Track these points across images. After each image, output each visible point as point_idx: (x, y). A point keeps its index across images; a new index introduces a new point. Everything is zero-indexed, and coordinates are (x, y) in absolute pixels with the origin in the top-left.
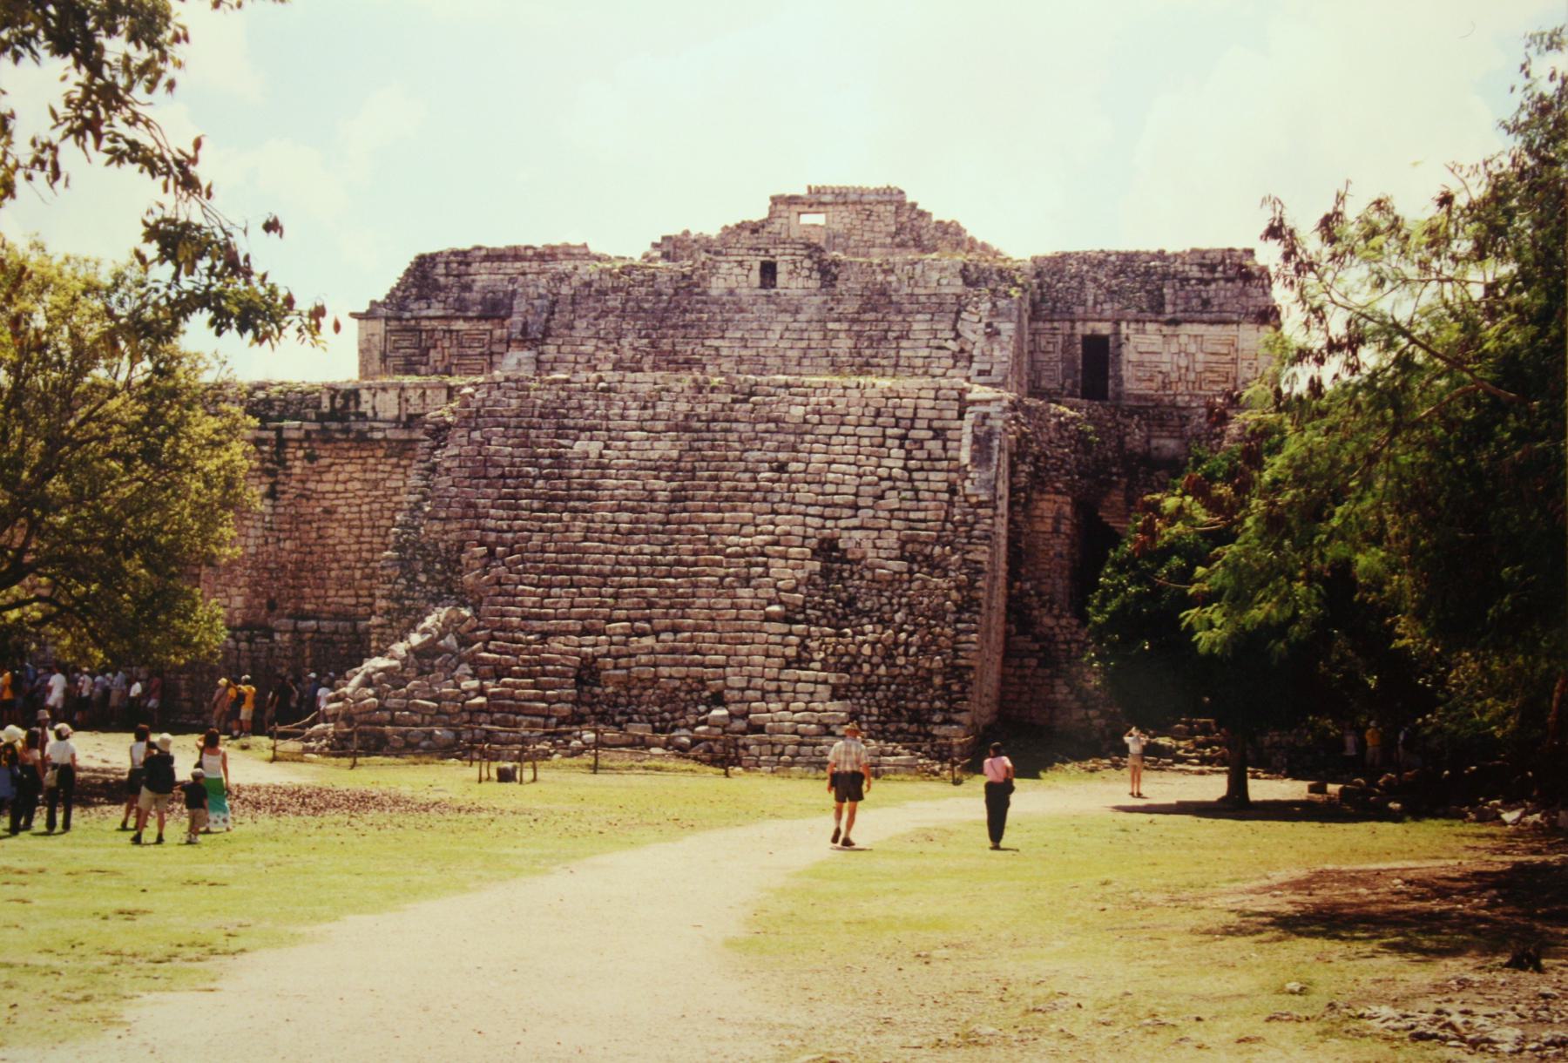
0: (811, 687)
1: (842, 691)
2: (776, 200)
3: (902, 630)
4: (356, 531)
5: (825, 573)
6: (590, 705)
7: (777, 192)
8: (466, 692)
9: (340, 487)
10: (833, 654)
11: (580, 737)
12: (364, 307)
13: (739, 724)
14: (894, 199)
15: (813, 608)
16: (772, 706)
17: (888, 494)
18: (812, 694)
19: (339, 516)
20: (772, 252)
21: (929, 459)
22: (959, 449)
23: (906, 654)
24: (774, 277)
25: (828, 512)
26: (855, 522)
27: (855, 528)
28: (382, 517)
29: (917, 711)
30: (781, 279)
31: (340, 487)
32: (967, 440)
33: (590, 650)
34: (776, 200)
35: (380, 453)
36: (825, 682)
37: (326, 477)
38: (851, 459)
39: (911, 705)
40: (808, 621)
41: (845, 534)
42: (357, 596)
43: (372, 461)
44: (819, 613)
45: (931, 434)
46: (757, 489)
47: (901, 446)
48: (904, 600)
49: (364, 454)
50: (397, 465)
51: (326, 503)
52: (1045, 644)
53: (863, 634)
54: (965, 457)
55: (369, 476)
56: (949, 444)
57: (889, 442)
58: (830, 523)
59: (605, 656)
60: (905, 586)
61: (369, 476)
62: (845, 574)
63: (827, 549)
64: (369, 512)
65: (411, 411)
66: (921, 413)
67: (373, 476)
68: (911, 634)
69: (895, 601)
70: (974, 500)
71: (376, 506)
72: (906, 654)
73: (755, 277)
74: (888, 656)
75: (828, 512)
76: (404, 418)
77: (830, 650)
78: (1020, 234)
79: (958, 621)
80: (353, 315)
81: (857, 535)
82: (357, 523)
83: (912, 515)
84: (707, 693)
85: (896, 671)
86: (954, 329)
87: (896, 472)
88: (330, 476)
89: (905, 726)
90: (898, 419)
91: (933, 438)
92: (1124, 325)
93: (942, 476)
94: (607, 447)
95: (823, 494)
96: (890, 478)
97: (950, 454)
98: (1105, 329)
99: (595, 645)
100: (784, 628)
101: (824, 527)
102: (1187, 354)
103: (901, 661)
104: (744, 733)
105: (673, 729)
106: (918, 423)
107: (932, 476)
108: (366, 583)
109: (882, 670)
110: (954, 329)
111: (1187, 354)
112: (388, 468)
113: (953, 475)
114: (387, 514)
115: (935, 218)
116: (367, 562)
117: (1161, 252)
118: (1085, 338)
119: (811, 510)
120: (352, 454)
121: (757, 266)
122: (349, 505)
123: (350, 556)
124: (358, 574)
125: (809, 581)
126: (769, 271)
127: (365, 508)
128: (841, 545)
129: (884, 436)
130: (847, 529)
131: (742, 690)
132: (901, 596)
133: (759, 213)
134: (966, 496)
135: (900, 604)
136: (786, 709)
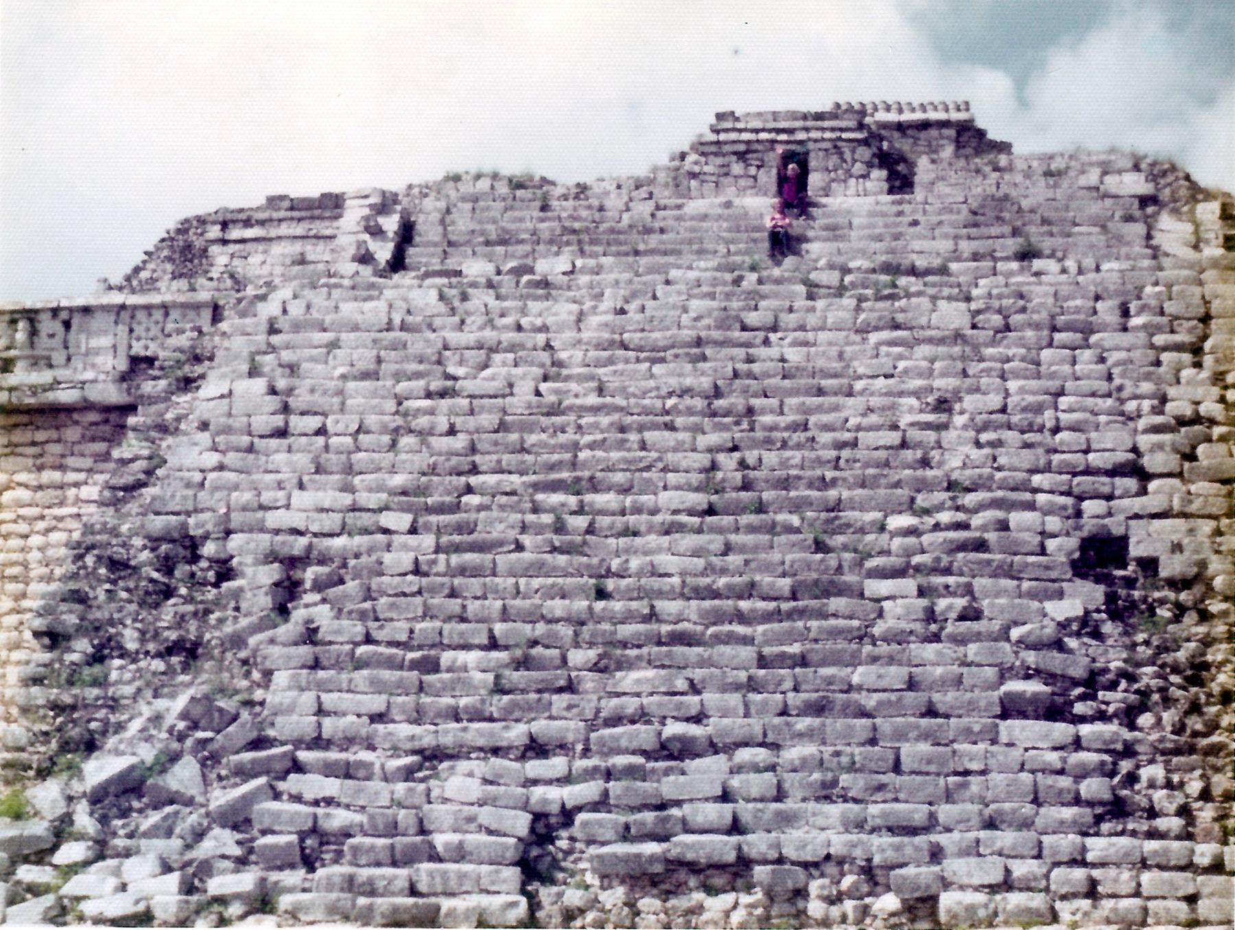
17: (1201, 450)
18: (1192, 899)
46: (904, 445)
47: (1198, 365)
49: (40, 436)
61: (50, 476)
63: (1100, 555)
81: (1172, 528)
112: (88, 462)
119: (1037, 480)
125: (1087, 626)
127: (36, 540)
129: (1152, 346)
130: (1137, 516)
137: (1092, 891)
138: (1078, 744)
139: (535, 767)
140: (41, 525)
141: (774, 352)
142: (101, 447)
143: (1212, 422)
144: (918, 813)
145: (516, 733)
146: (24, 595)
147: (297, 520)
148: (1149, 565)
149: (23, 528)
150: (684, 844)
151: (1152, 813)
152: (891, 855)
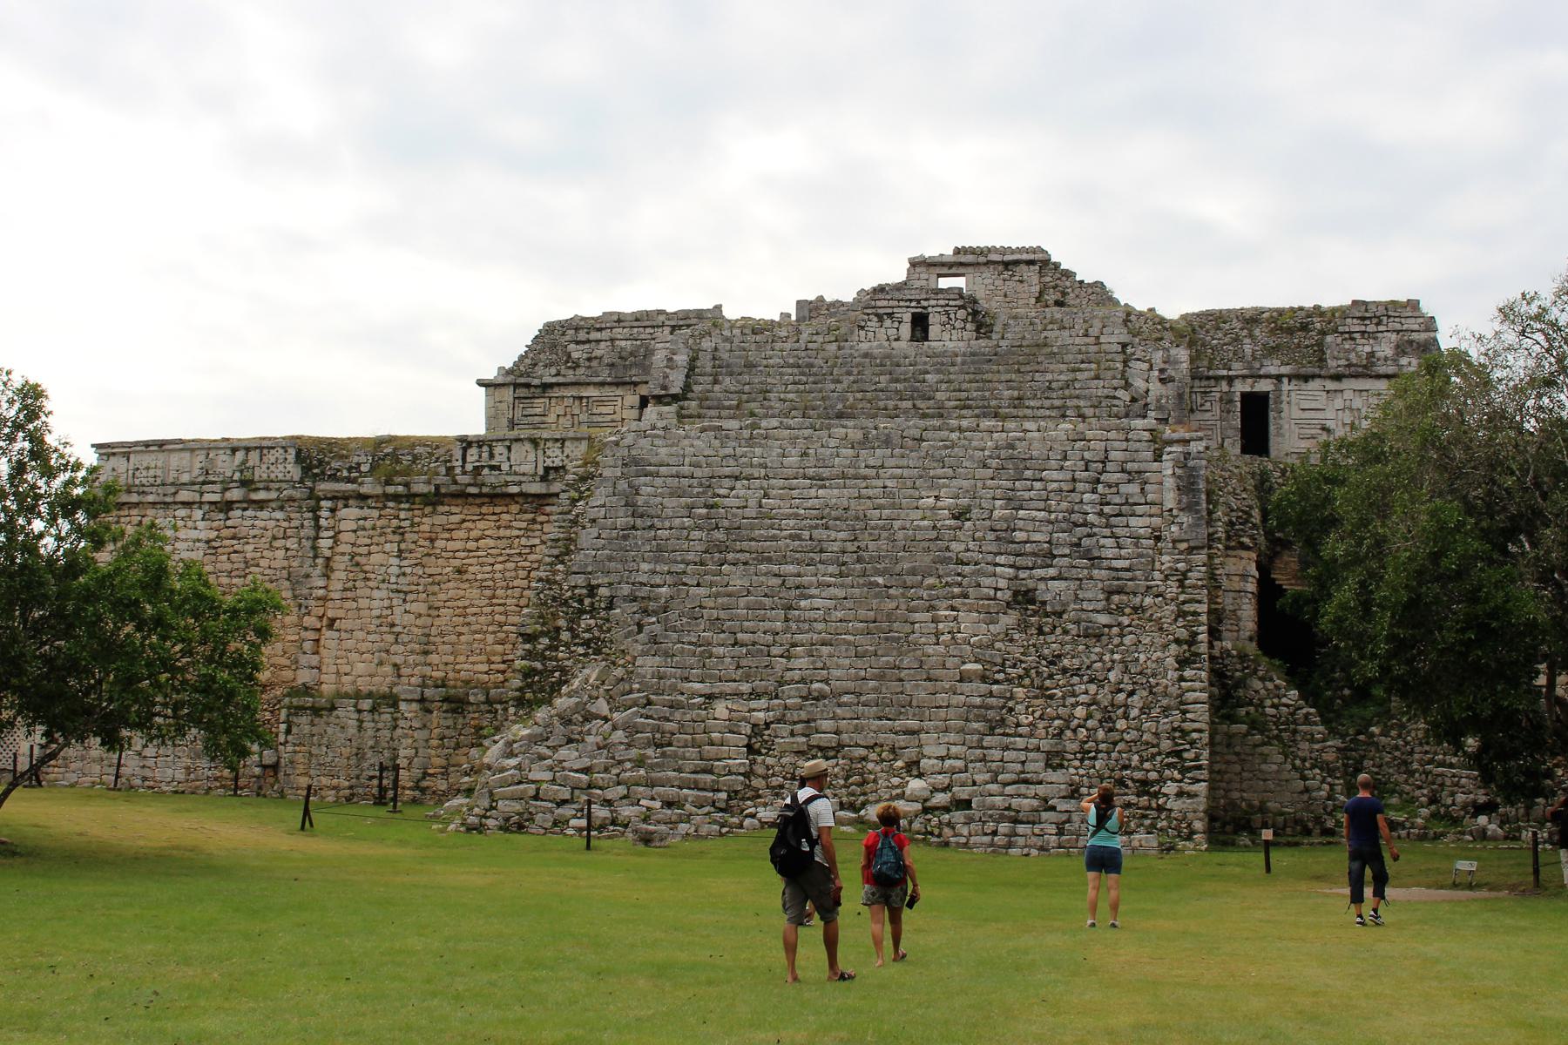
0: (1022, 756)
1: (1056, 761)
2: (915, 264)
3: (1121, 691)
4: (488, 593)
5: (1023, 626)
6: (766, 777)
7: (915, 253)
8: (620, 762)
9: (472, 545)
10: (1041, 718)
11: (753, 816)
12: (491, 374)
13: (940, 799)
14: (1039, 262)
15: (1014, 666)
16: (979, 778)
19: (471, 577)
20: (924, 303)
21: (1127, 503)
22: (1161, 492)
23: (1126, 716)
24: (926, 331)
25: (1020, 561)
26: (1052, 572)
27: (1053, 579)
28: (517, 577)
29: (1145, 783)
30: (934, 331)
31: (472, 545)
32: (1170, 483)
33: (761, 715)
34: (915, 264)
35: (515, 508)
36: (1038, 749)
37: (456, 534)
38: (1041, 505)
39: (1138, 775)
40: (1009, 680)
41: (1042, 586)
42: (490, 662)
43: (505, 517)
44: (1021, 672)
45: (1126, 476)
47: (1094, 491)
48: (1117, 657)
49: (498, 510)
50: (534, 521)
51: (457, 563)
53: (1074, 695)
54: (1170, 500)
55: (502, 532)
56: (1147, 487)
57: (1080, 486)
58: (1022, 574)
59: (779, 721)
60: (1116, 641)
61: (502, 532)
62: (1046, 629)
63: (1023, 598)
64: (503, 572)
65: (549, 463)
66: (1113, 455)
67: (508, 533)
68: (1131, 694)
69: (1107, 658)
70: (1183, 546)
71: (510, 565)
72: (1126, 716)
73: (906, 330)
74: (1107, 720)
75: (1020, 561)
76: (541, 471)
77: (1037, 714)
78: (1168, 289)
79: (1182, 679)
80: (481, 383)
82: (490, 583)
83: (1115, 564)
84: (899, 764)
85: (1115, 736)
86: (1123, 377)
87: (1091, 518)
88: (461, 534)
89: (1133, 799)
90: (1087, 463)
91: (1129, 481)
92: (1285, 380)
93: (1146, 521)
94: (766, 496)
95: (1013, 542)
96: (1085, 524)
97: (1150, 497)
98: (1264, 386)
99: (768, 710)
100: (984, 687)
101: (1016, 577)
102: (1351, 409)
103: (1121, 724)
104: (947, 809)
105: (864, 805)
106: (1110, 466)
107: (1133, 521)
108: (499, 648)
109: (1101, 734)
110: (1123, 377)
111: (1351, 409)
112: (524, 525)
113: (1156, 521)
114: (522, 574)
115: (1078, 278)
116: (501, 625)
117: (1317, 307)
118: (1244, 395)
119: (1001, 559)
120: (484, 510)
121: (907, 317)
122: (482, 565)
123: (482, 619)
124: (490, 638)
126: (920, 324)
127: (498, 567)
128: (1040, 595)
129: (1074, 480)
130: (1042, 579)
131: (942, 759)
132: (1113, 653)
133: (896, 273)
134: (1174, 542)
135: (1113, 661)
136: (994, 781)
137: (983, 760)
138: (991, 694)
139: (754, 704)
140: (501, 559)
141: (880, 483)
142: (531, 516)
143: (1093, 525)
144: (913, 724)
145: (745, 687)
146: (494, 597)
147: (644, 579)
148: (1044, 603)
149: (491, 560)
150: (816, 739)
151: (1018, 725)
152: (903, 744)
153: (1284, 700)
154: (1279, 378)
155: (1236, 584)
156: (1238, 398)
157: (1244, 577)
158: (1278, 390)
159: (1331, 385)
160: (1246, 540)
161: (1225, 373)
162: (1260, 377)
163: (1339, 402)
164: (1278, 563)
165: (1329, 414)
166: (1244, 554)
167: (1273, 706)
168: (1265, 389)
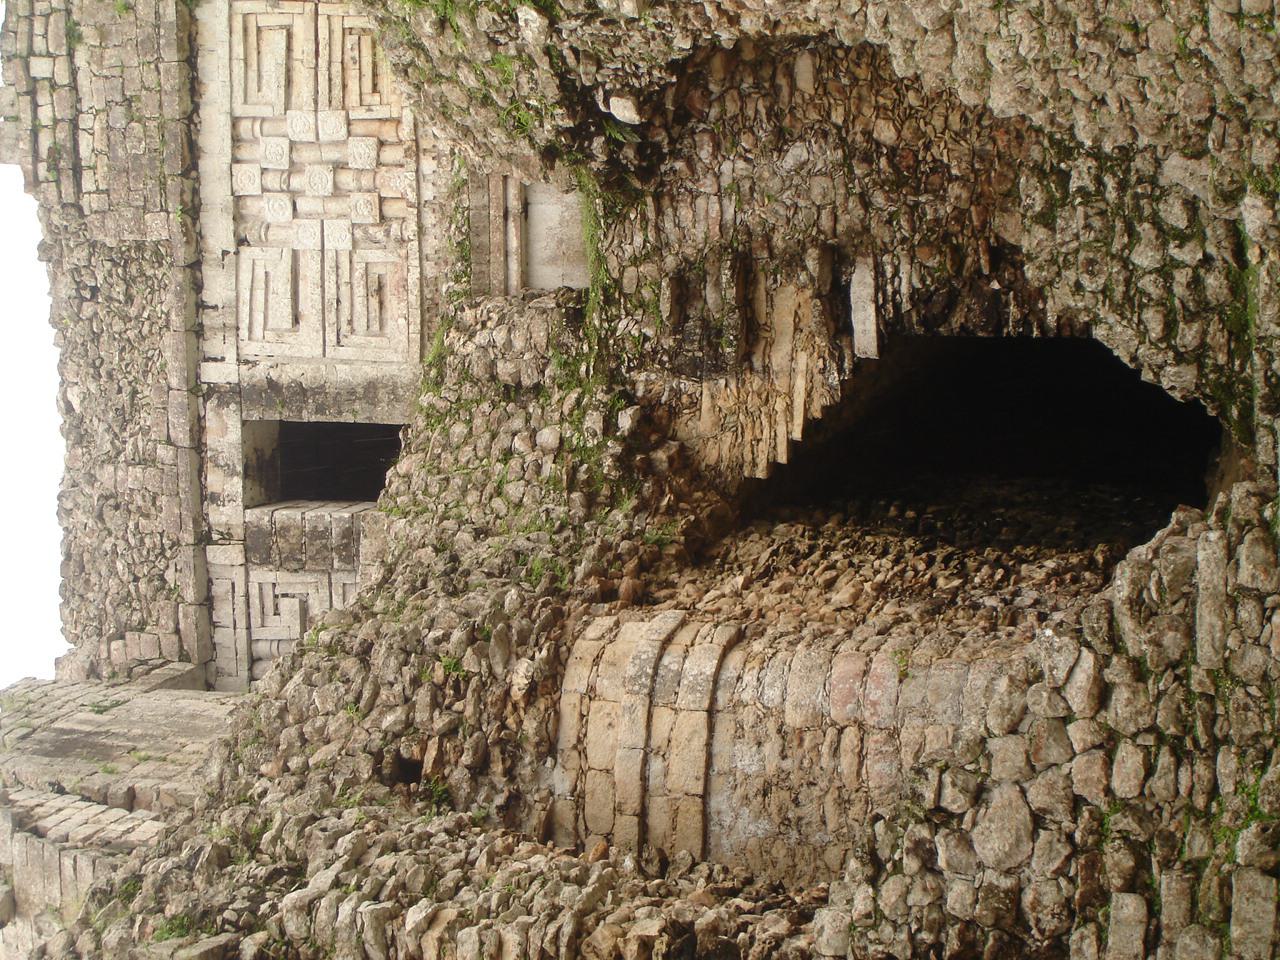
52: (1117, 860)
92: (211, 373)
98: (226, 434)
102: (294, 167)
111: (294, 167)
153: (1078, 696)
154: (199, 391)
155: (682, 725)
156: (260, 516)
157: (654, 689)
158: (236, 394)
159: (218, 232)
160: (521, 675)
161: (186, 554)
162: (198, 445)
163: (272, 210)
164: (717, 451)
165: (306, 237)
166: (576, 678)
167: (1108, 744)
168: (235, 434)
